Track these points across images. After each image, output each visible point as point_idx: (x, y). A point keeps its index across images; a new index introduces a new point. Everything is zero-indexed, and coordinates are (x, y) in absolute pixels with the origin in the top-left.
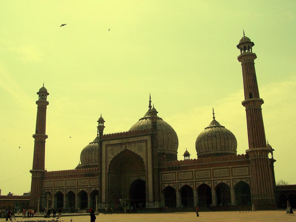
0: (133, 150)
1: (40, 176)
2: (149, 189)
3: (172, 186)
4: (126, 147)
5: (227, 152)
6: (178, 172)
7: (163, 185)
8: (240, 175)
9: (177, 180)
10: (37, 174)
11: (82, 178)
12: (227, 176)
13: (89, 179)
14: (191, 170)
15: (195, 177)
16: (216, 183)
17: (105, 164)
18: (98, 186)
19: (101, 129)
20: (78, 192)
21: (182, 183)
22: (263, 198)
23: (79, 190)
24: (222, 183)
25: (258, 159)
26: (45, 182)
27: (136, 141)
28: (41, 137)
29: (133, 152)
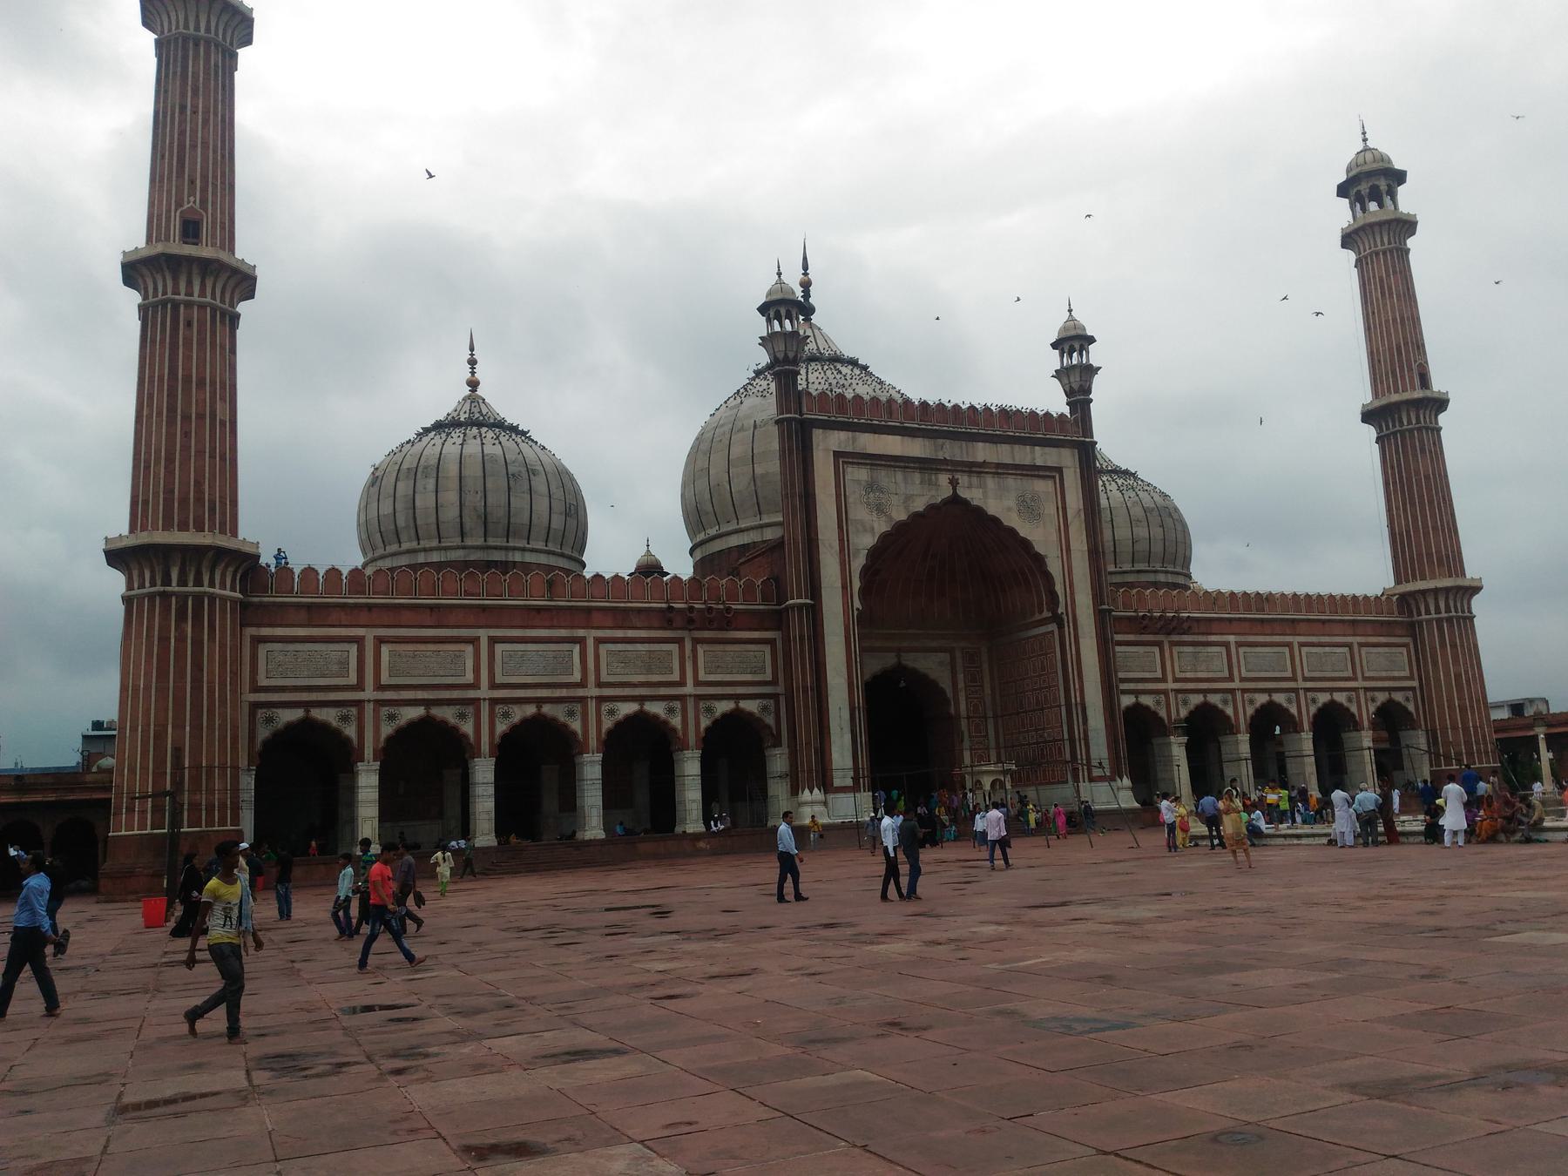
0: (993, 507)
2: (1090, 713)
3: (1153, 708)
4: (954, 483)
6: (1173, 644)
8: (1384, 674)
11: (631, 633)
12: (1345, 674)
16: (1314, 701)
20: (608, 724)
22: (1492, 765)
23: (612, 712)
24: (1333, 703)
26: (262, 650)
28: (232, 283)
29: (995, 521)
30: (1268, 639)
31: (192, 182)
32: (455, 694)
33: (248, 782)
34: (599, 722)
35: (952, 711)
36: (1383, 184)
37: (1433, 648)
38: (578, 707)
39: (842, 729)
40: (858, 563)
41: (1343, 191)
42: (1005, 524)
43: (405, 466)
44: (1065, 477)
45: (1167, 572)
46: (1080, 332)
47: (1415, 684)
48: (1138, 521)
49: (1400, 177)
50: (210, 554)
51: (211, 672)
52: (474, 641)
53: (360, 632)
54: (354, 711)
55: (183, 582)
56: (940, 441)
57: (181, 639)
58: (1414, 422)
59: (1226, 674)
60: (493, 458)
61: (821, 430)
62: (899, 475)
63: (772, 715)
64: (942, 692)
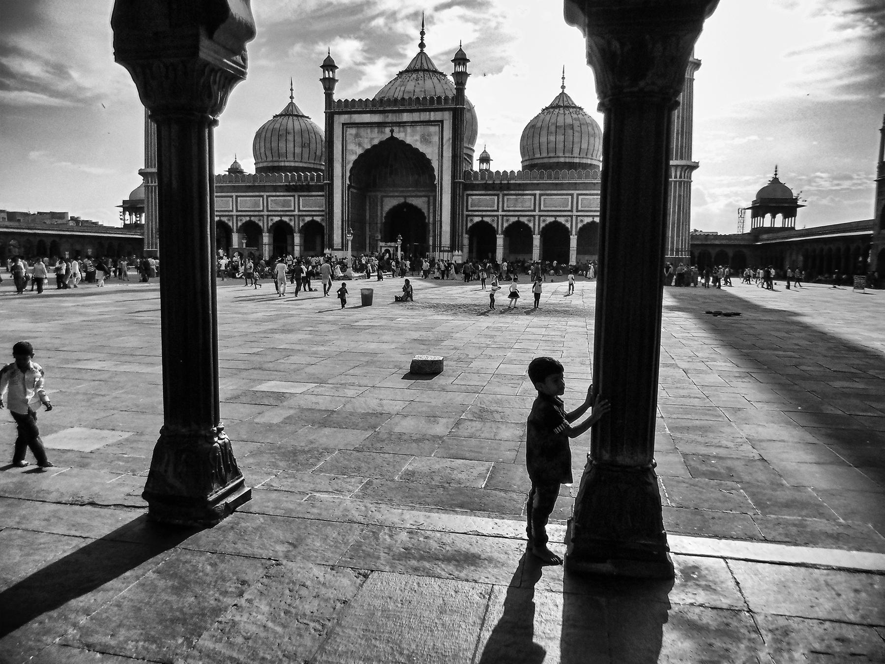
0: (409, 140)
4: (392, 131)
5: (589, 162)
6: (504, 195)
7: (469, 219)
9: (500, 210)
11: (278, 194)
13: (296, 197)
16: (582, 221)
17: (341, 165)
18: (323, 213)
19: (329, 84)
20: (270, 224)
23: (272, 220)
27: (417, 119)
29: (410, 145)
32: (227, 213)
34: (268, 224)
35: (427, 221)
40: (349, 166)
45: (566, 157)
48: (551, 133)
52: (232, 197)
55: (152, 183)
57: (152, 198)
59: (532, 208)
60: (276, 128)
62: (369, 131)
64: (423, 213)
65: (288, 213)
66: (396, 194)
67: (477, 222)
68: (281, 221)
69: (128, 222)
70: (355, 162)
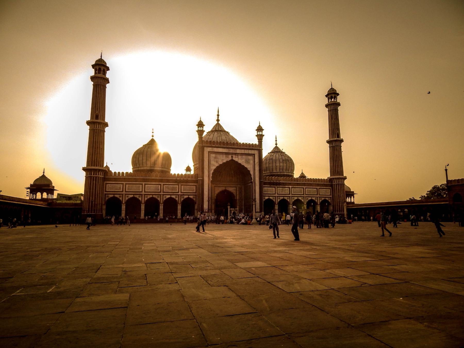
0: (240, 161)
1: (102, 175)
4: (232, 157)
6: (277, 187)
8: (324, 194)
10: (99, 174)
11: (169, 183)
14: (289, 186)
15: (292, 193)
16: (308, 199)
19: (200, 132)
20: (164, 199)
21: (295, 197)
23: (165, 197)
24: (312, 199)
25: (342, 184)
26: (107, 185)
29: (240, 164)
30: (299, 187)
31: (97, 109)
32: (138, 193)
33: (104, 207)
35: (236, 198)
36: (333, 95)
37: (335, 189)
38: (159, 196)
39: (206, 201)
41: (326, 96)
42: (242, 164)
43: (138, 152)
44: (255, 156)
46: (261, 128)
47: (331, 196)
48: (281, 162)
49: (338, 94)
50: (98, 170)
51: (98, 189)
52: (142, 184)
53: (123, 182)
54: (121, 195)
55: (94, 175)
56: (230, 149)
57: (93, 184)
58: (335, 144)
59: (289, 193)
61: (206, 148)
62: (221, 155)
63: (195, 198)
64: (234, 195)
65: (175, 194)
66: (221, 186)
67: (267, 199)
68: (171, 198)
69: (31, 198)
70: (215, 170)
